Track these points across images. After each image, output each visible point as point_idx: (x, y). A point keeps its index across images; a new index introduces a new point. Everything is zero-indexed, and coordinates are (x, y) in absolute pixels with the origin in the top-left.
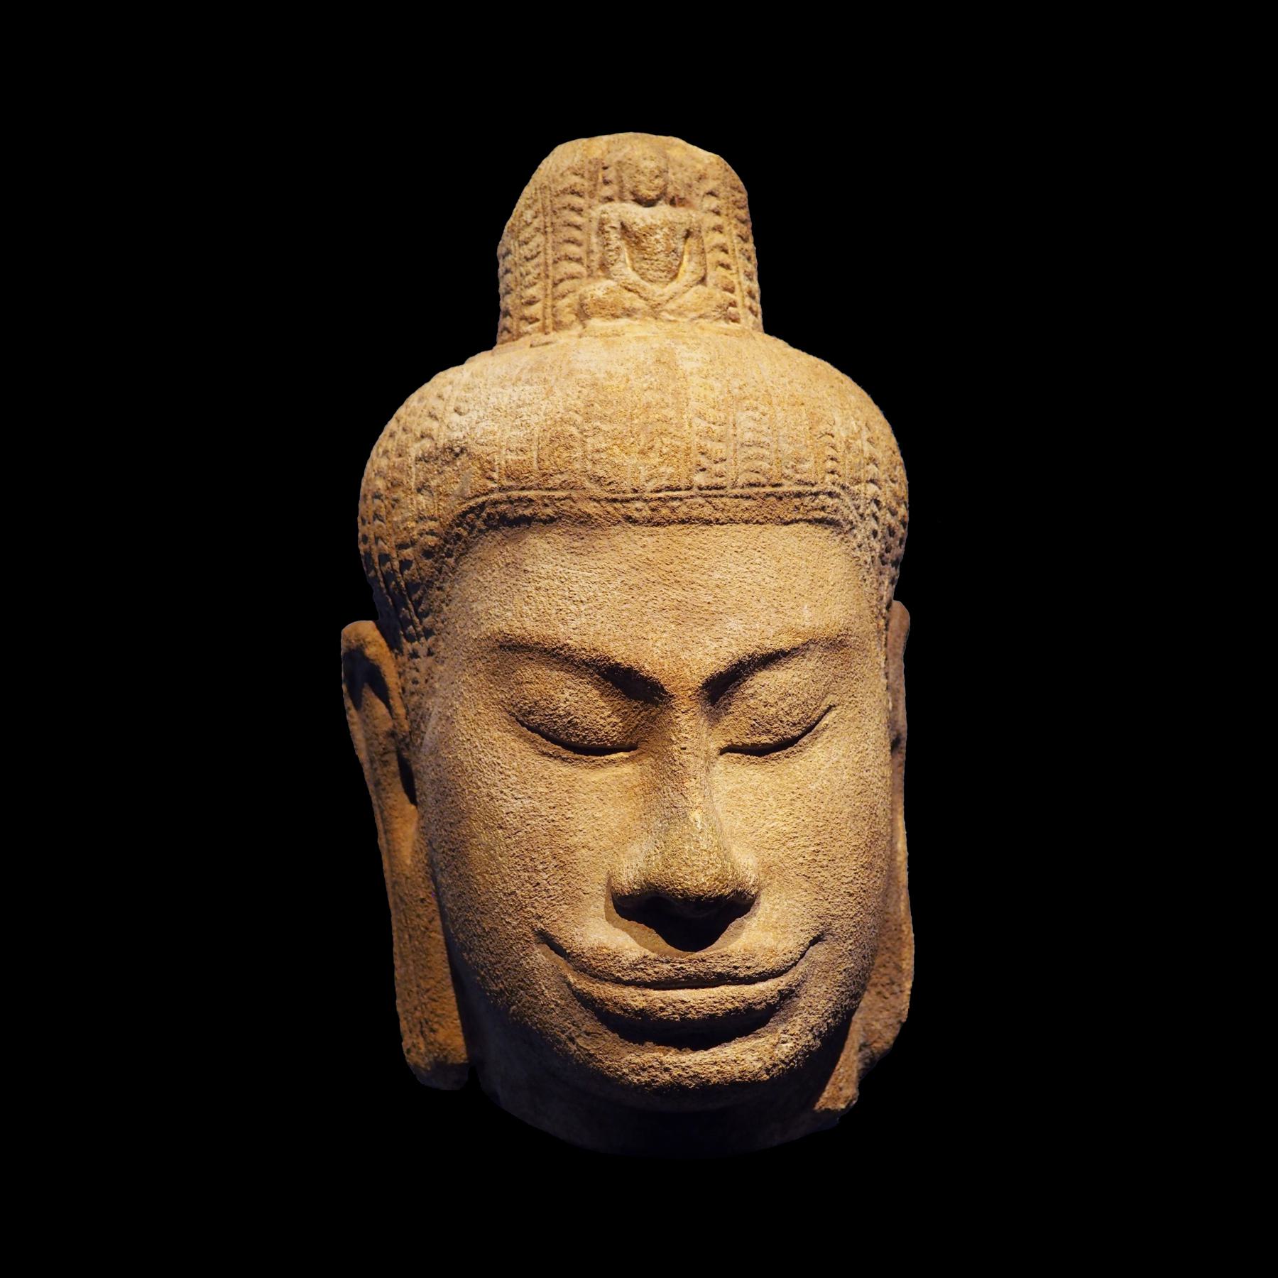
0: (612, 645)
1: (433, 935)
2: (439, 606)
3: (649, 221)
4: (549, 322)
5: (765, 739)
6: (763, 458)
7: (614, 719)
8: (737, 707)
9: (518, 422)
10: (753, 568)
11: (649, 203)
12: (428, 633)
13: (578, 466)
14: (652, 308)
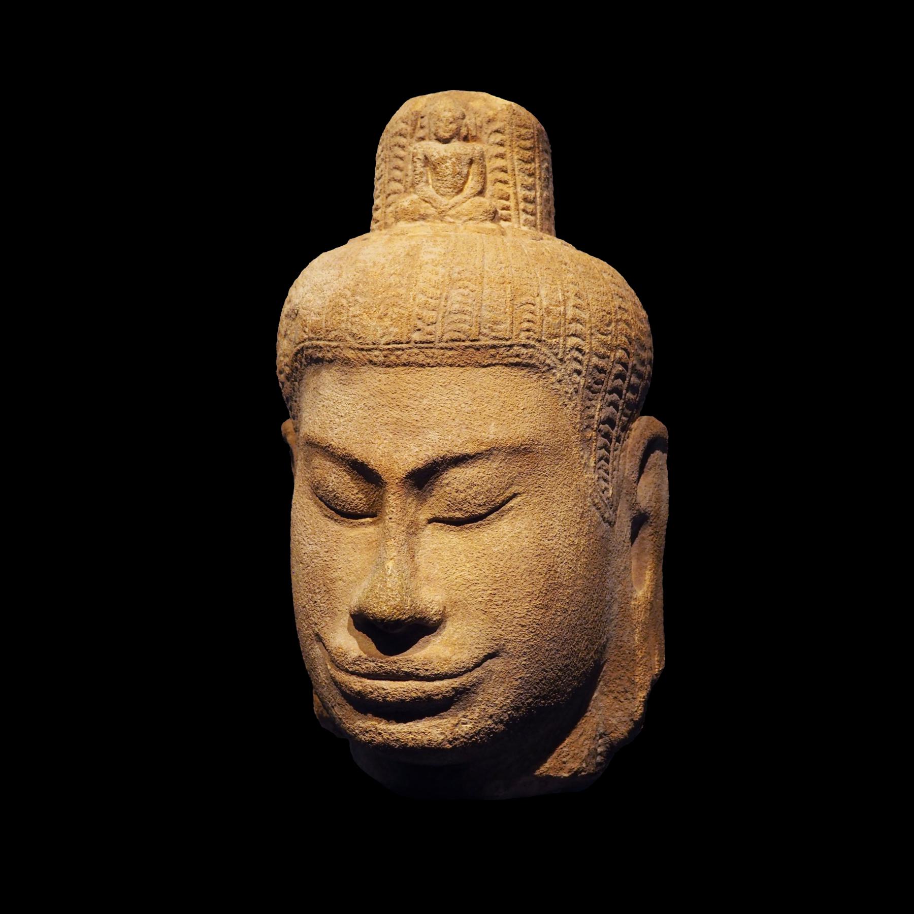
0: (354, 446)
3: (443, 153)
5: (458, 515)
7: (360, 496)
8: (438, 492)
10: (452, 397)
11: (446, 141)
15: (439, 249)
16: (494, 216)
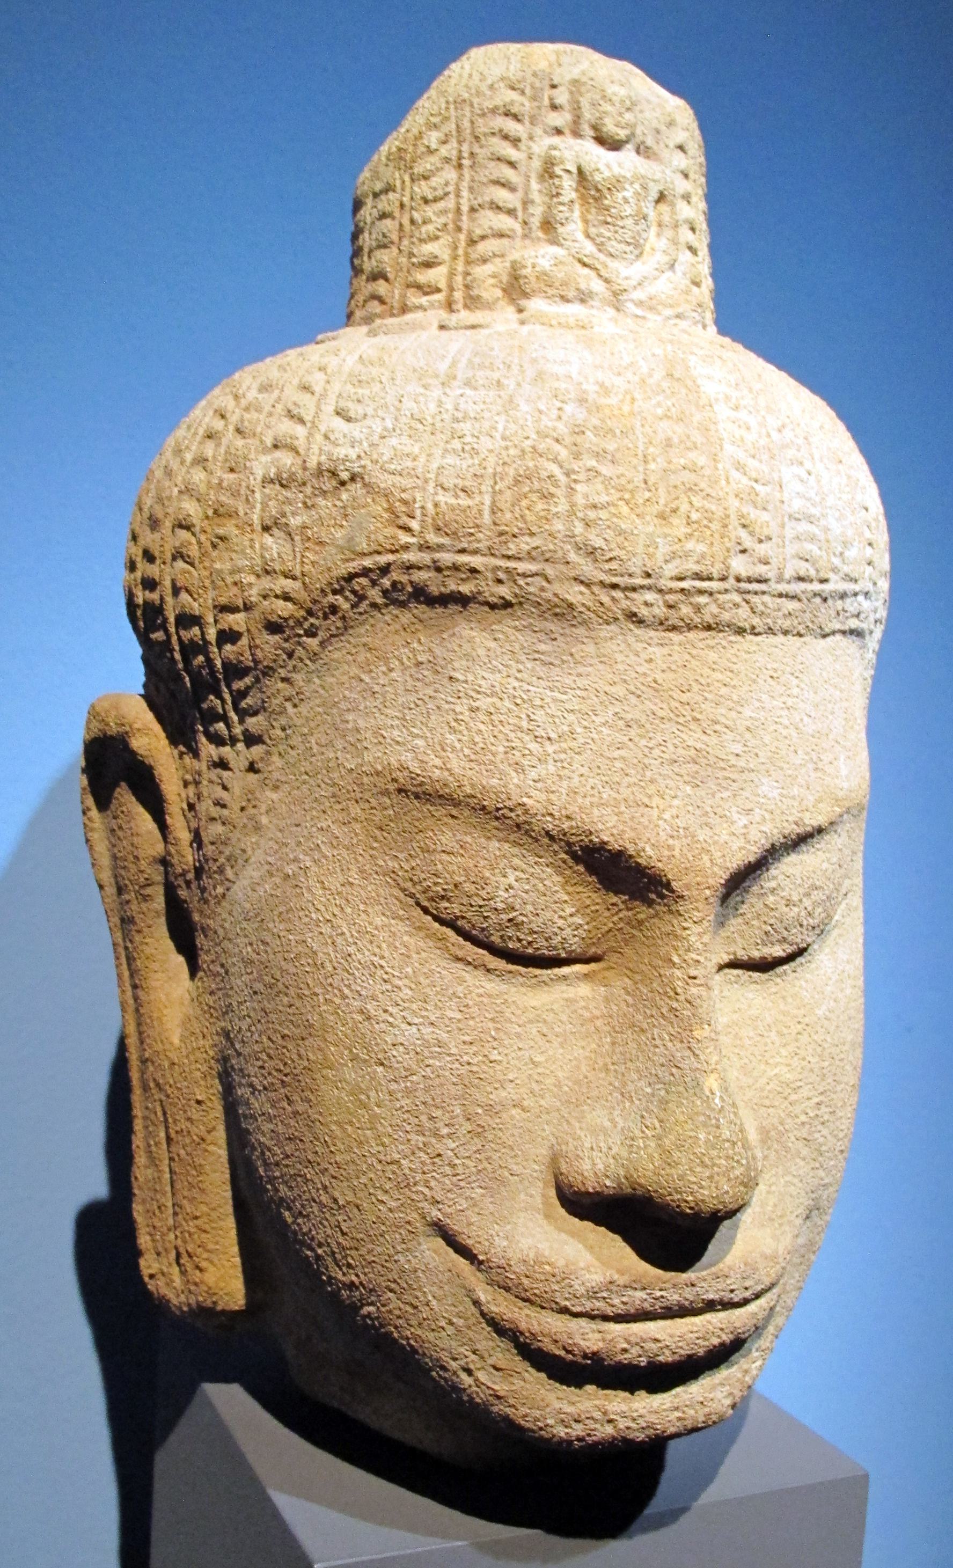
0: (596, 812)
1: (212, 1148)
2: (281, 705)
3: (617, 171)
4: (458, 295)
5: (778, 951)
6: (812, 539)
7: (578, 920)
9: (456, 444)
10: (790, 702)
12: (252, 740)
13: (560, 527)
14: (615, 294)
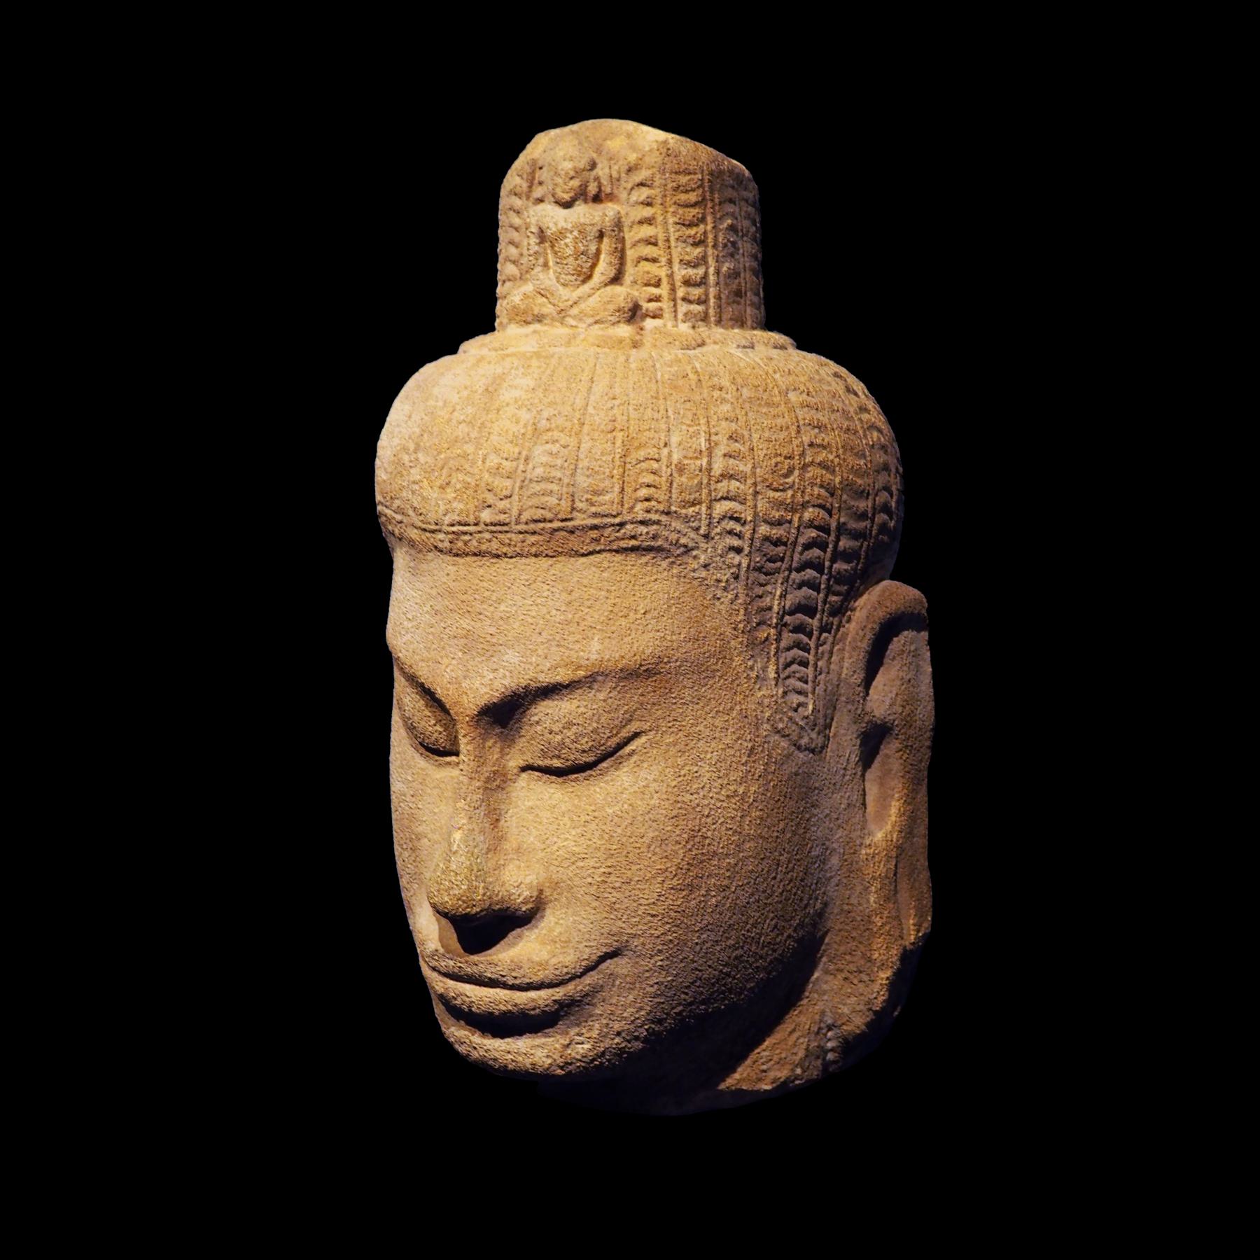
3: (562, 224)
5: (557, 763)
8: (527, 732)
10: (539, 601)
11: (567, 205)
15: (529, 382)
16: (634, 314)
